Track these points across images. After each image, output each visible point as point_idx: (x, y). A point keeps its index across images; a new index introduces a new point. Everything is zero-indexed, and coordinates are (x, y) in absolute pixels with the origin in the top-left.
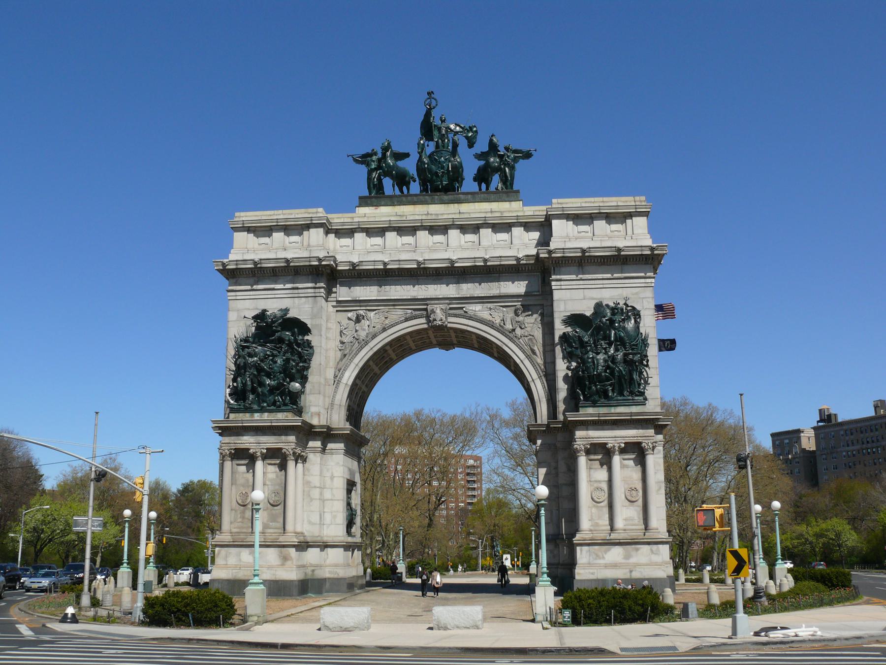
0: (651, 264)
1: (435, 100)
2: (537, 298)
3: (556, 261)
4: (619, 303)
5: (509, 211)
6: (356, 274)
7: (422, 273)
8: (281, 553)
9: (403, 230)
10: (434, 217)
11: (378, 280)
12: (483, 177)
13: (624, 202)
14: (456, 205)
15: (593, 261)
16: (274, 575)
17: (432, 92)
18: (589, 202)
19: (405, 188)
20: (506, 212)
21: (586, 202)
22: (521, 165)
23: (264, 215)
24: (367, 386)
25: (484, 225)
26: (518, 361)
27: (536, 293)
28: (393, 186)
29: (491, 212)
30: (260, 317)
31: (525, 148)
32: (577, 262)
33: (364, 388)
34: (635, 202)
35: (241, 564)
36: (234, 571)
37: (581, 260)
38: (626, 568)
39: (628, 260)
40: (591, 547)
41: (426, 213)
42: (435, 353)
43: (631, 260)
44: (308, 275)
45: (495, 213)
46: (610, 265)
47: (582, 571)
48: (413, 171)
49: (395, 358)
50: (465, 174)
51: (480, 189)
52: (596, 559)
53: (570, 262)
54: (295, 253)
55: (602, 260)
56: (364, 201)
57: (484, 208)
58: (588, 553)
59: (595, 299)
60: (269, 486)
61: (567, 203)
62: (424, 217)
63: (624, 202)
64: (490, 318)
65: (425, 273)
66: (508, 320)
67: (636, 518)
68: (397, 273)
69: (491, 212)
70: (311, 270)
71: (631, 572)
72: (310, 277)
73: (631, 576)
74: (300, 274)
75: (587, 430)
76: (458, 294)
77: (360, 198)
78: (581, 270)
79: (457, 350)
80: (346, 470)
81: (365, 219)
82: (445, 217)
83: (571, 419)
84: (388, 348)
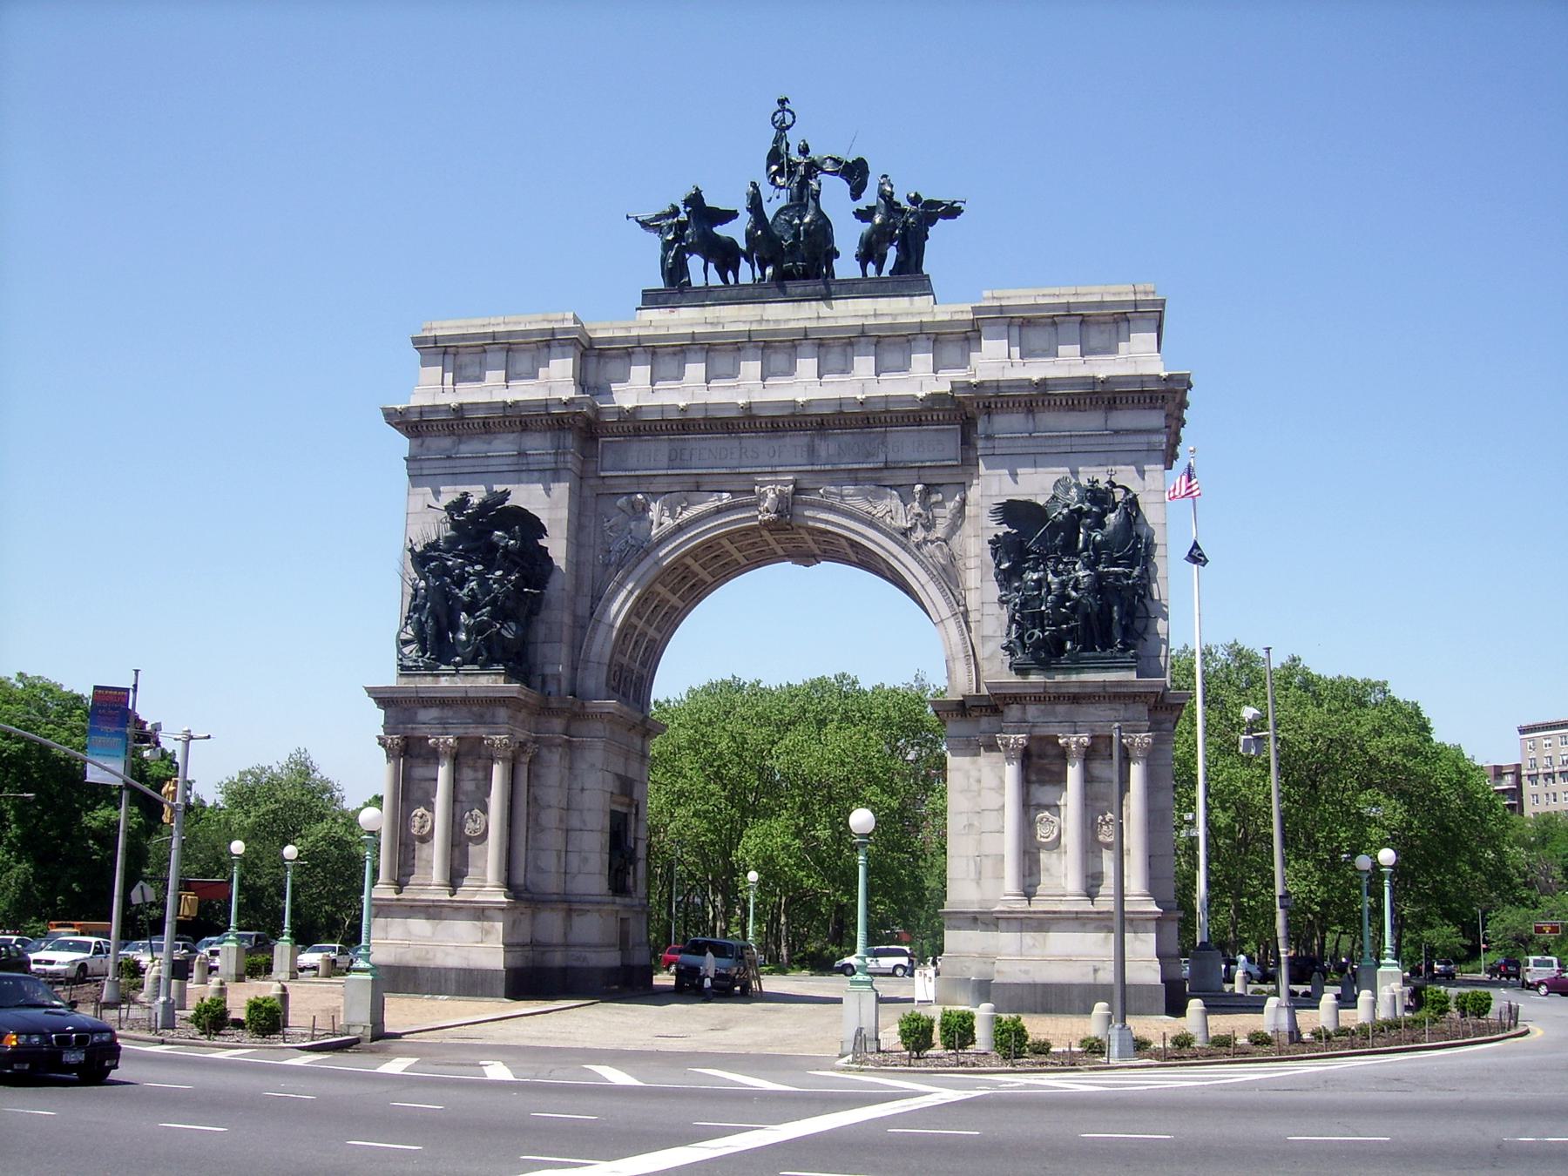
0: (1162, 408)
1: (792, 113)
2: (954, 471)
4: (1097, 481)
5: (907, 314)
6: (631, 428)
7: (747, 426)
9: (716, 350)
10: (772, 326)
11: (671, 440)
12: (870, 252)
13: (1114, 294)
14: (814, 303)
15: (1052, 403)
16: (466, 958)
17: (787, 99)
18: (1050, 295)
19: (730, 275)
20: (901, 314)
21: (1044, 295)
22: (939, 232)
23: (472, 326)
24: (658, 629)
25: (862, 339)
27: (950, 463)
28: (706, 269)
29: (875, 315)
30: (461, 503)
31: (945, 197)
32: (1023, 404)
33: (651, 632)
34: (1135, 293)
37: (1031, 401)
39: (1118, 402)
41: (759, 318)
42: (783, 573)
43: (1124, 401)
44: (545, 431)
45: (881, 317)
48: (743, 245)
49: (710, 579)
50: (838, 244)
51: (865, 274)
53: (1011, 405)
54: (525, 392)
55: (1070, 403)
56: (651, 299)
57: (864, 307)
60: (464, 804)
61: (1008, 298)
62: (754, 327)
63: (1114, 294)
64: (866, 507)
65: (752, 426)
66: (900, 512)
68: (702, 427)
69: (875, 315)
70: (550, 422)
71: (1096, 971)
72: (548, 434)
73: (1095, 979)
74: (531, 430)
76: (813, 464)
77: (646, 294)
78: (1030, 417)
79: (825, 565)
80: (609, 778)
81: (651, 332)
82: (792, 325)
84: (689, 561)
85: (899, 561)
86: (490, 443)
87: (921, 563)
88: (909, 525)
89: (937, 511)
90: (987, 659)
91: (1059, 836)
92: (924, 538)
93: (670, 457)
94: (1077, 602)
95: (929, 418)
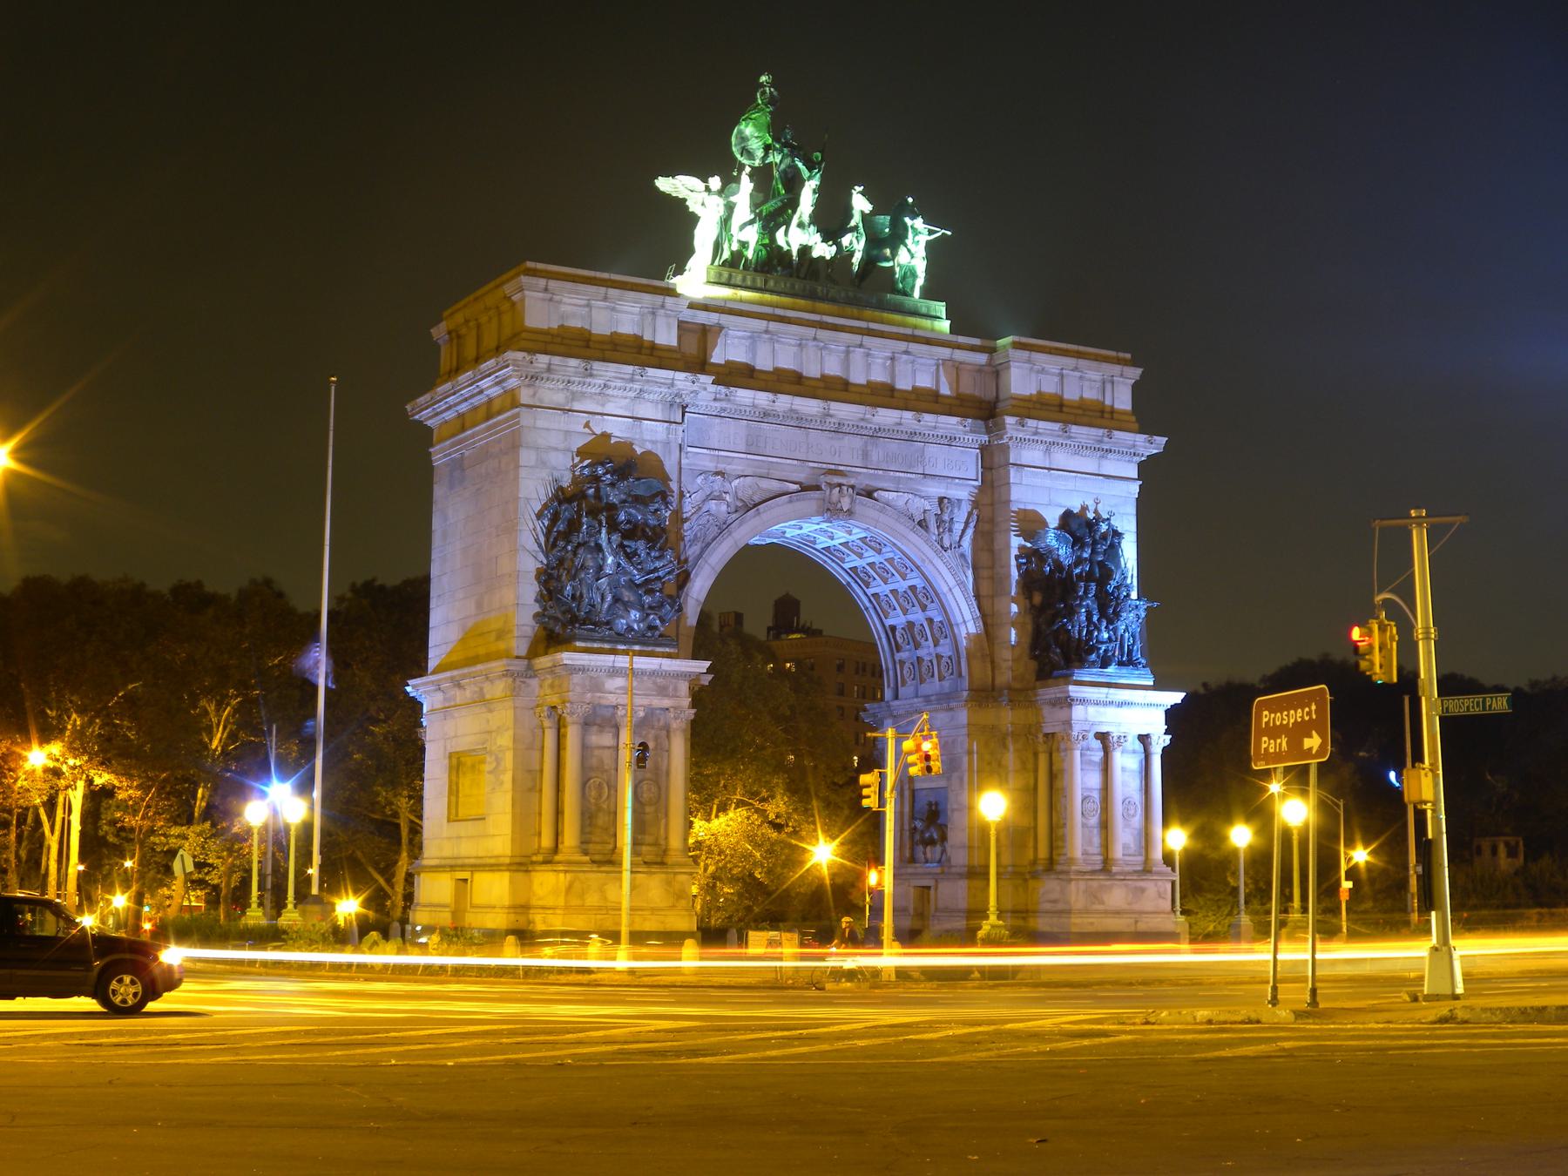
8: (669, 883)
16: (662, 923)
35: (609, 904)
36: (598, 916)
38: (1131, 918)
47: (1078, 921)
52: (1094, 903)
59: (1065, 507)
67: (1132, 846)
71: (1136, 922)
86: (603, 405)
93: (747, 441)
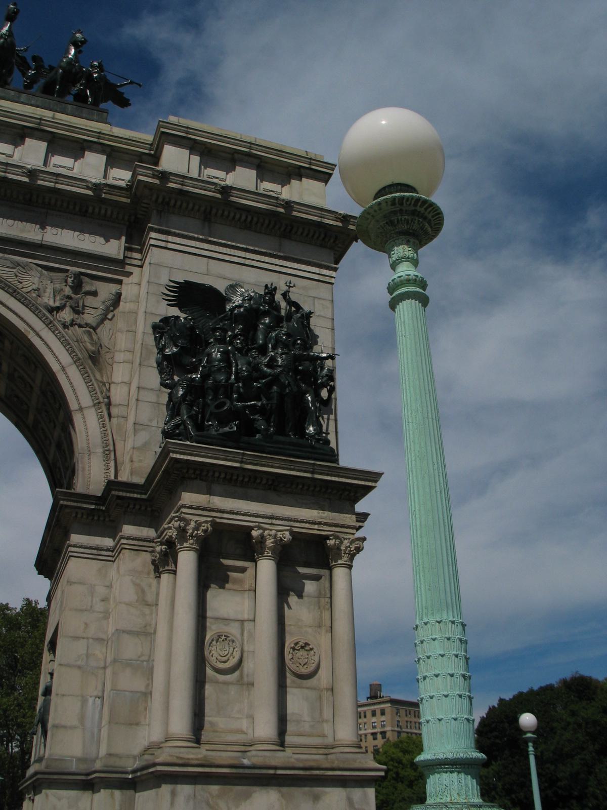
3: (164, 199)
26: (55, 367)
32: (203, 209)
40: (199, 787)
46: (260, 232)
55: (249, 219)
58: (191, 803)
75: (210, 492)
83: (178, 456)
85: (41, 338)
87: (66, 344)
88: (57, 304)
89: (89, 300)
90: (138, 448)
91: (241, 661)
92: (73, 320)
94: (275, 379)
95: (97, 210)
